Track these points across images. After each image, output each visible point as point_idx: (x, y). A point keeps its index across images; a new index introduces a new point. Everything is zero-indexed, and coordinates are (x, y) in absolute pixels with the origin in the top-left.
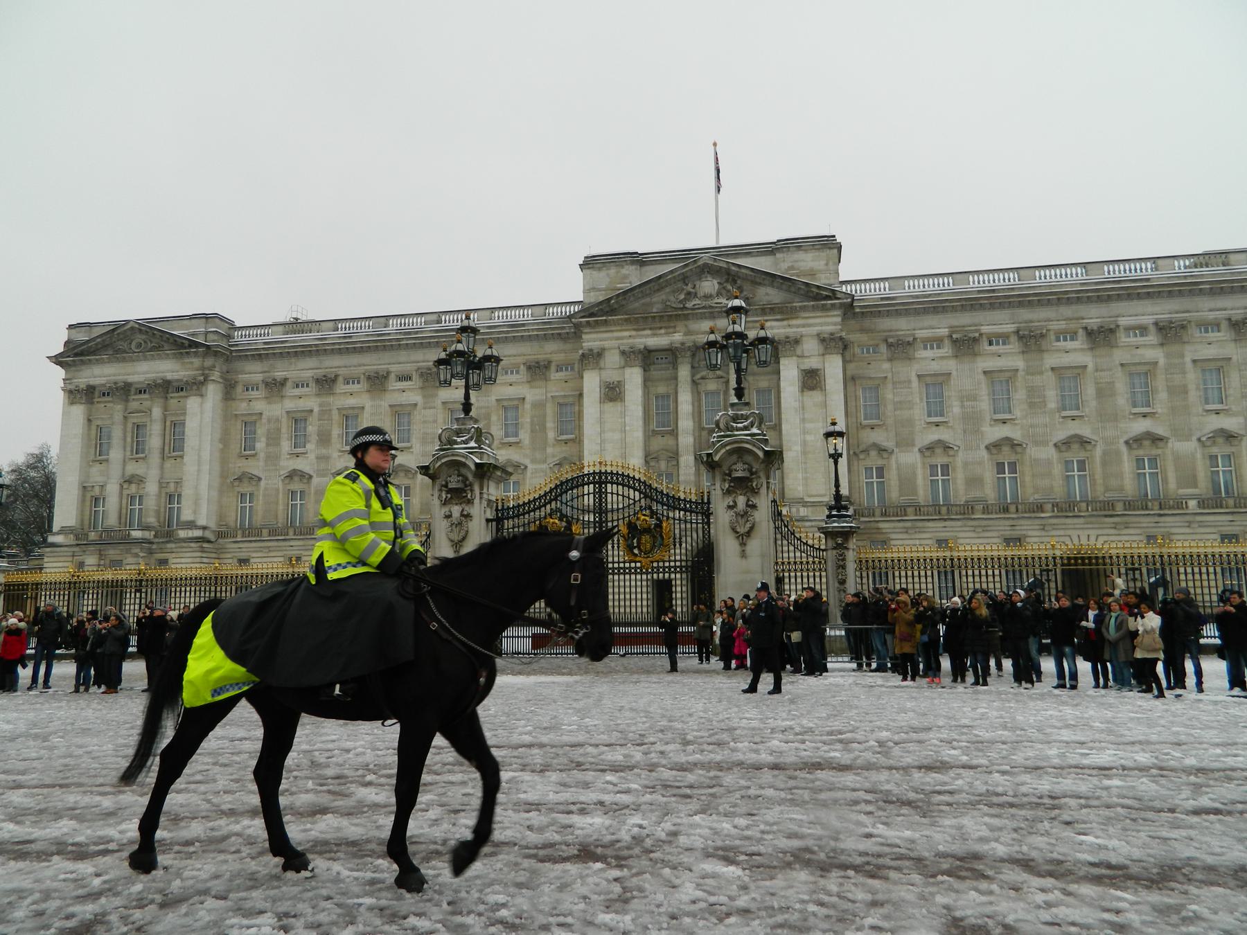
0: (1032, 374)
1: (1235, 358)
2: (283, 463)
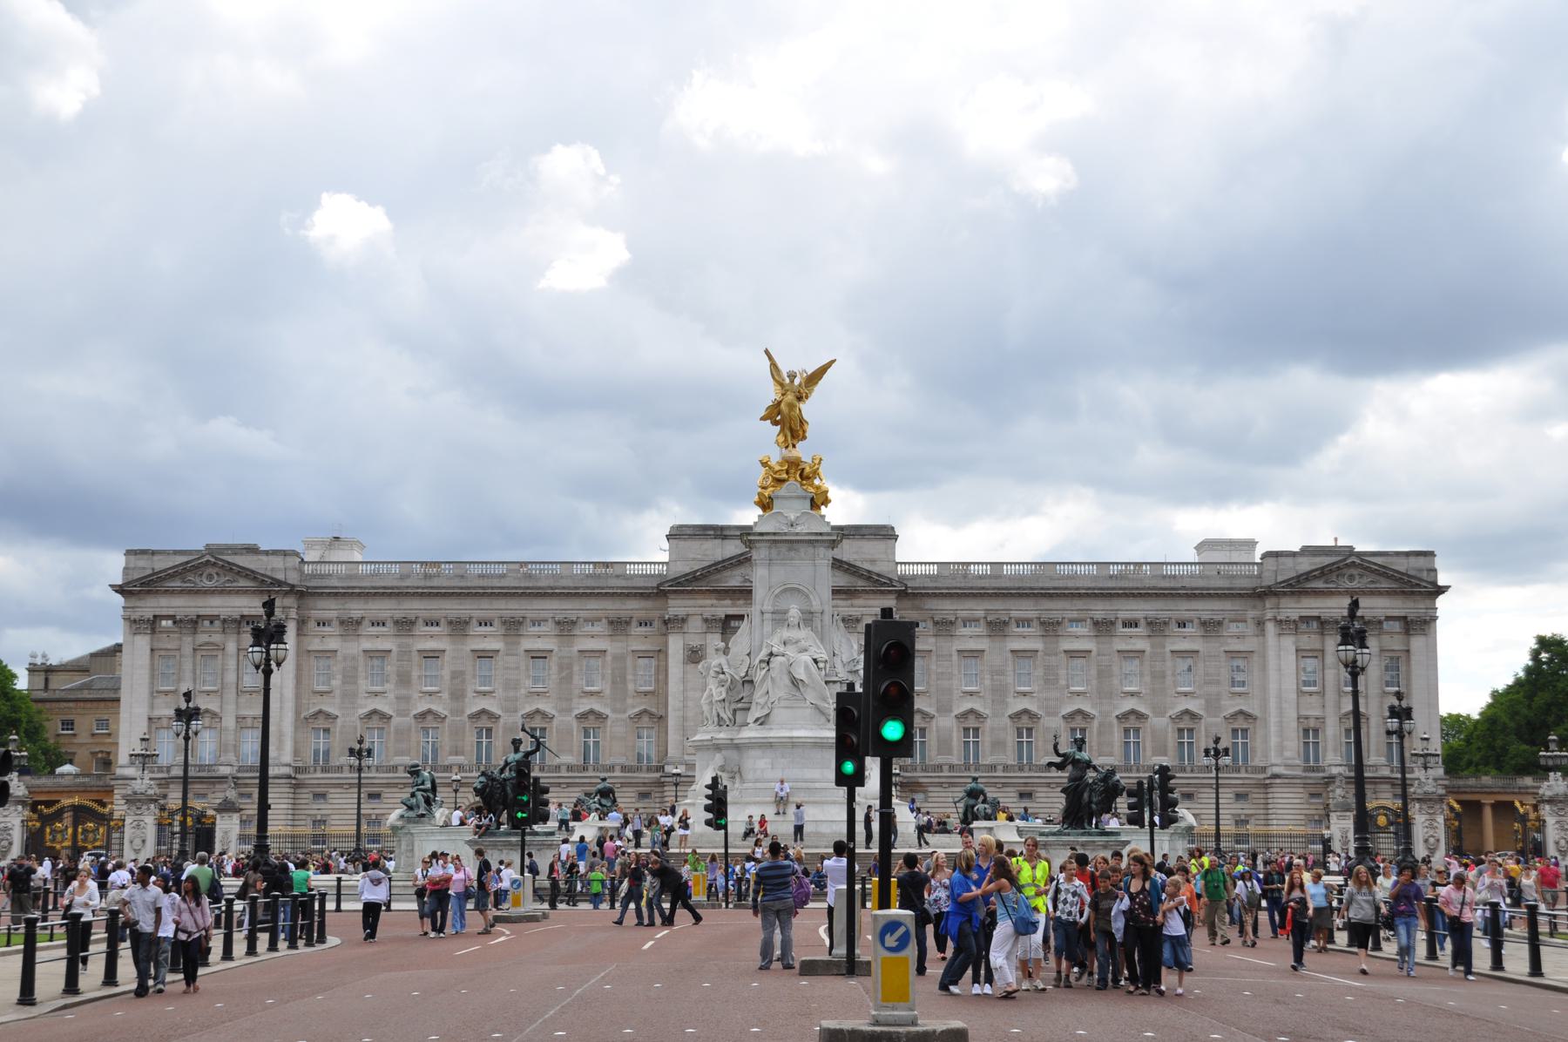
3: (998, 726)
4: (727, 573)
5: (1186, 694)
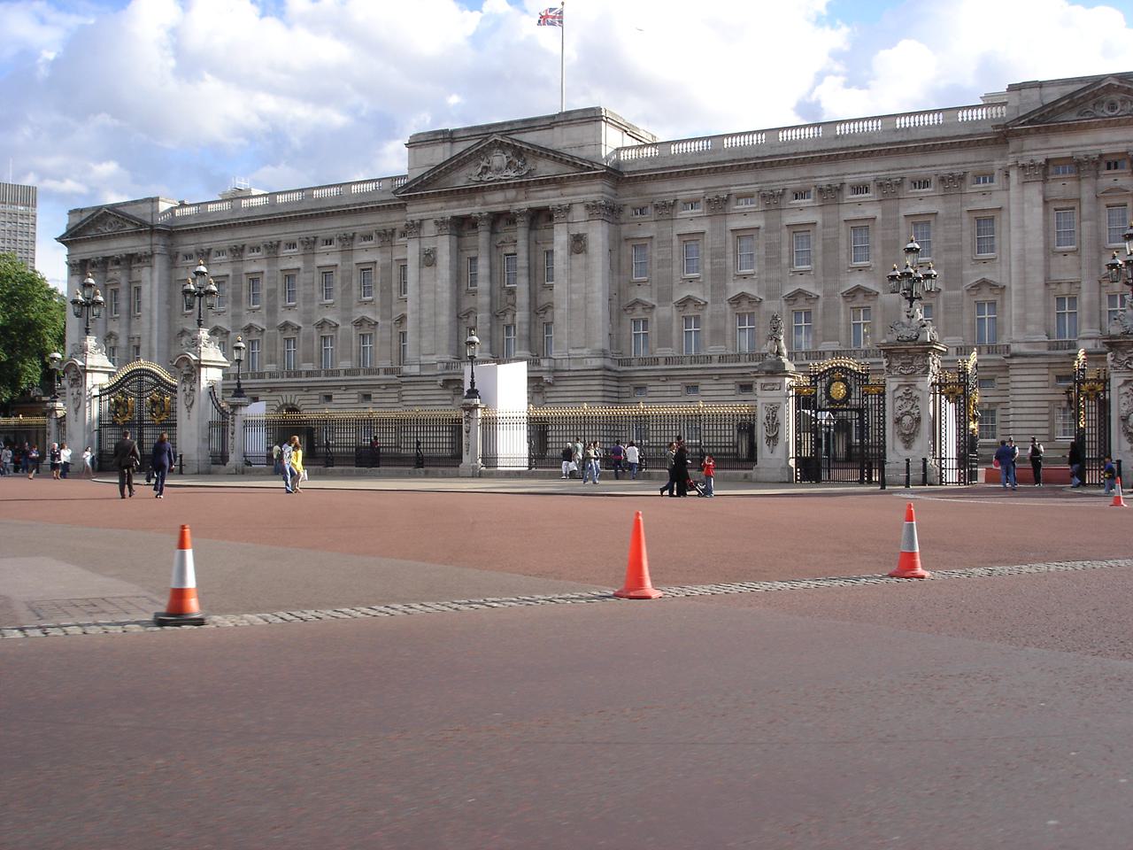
0: (770, 232)
1: (940, 212)
3: (717, 312)
4: (454, 175)
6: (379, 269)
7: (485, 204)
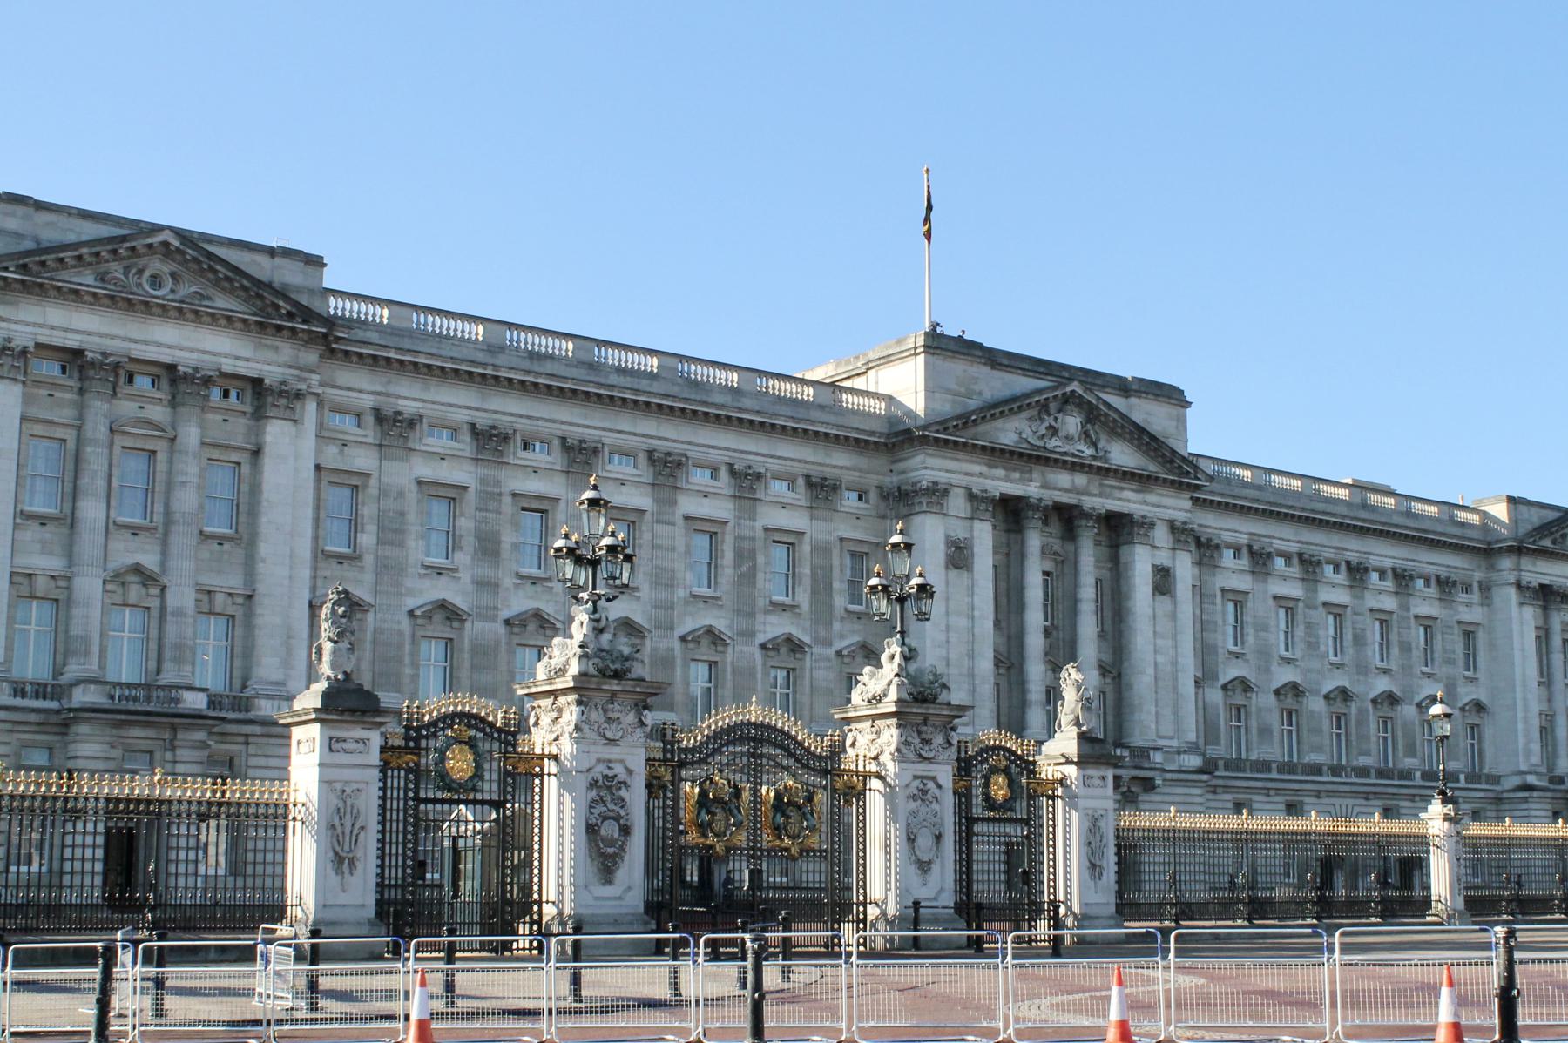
2: (409, 583)
3: (1264, 702)
4: (998, 423)
5: (1429, 676)
6: (806, 548)
7: (1044, 486)
